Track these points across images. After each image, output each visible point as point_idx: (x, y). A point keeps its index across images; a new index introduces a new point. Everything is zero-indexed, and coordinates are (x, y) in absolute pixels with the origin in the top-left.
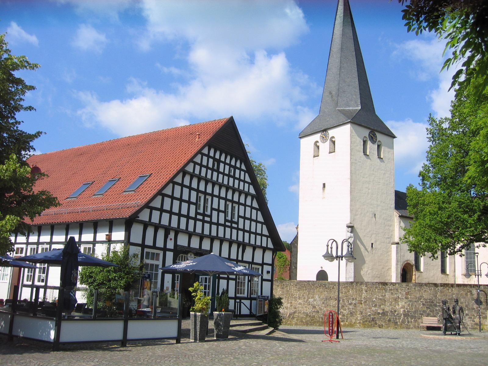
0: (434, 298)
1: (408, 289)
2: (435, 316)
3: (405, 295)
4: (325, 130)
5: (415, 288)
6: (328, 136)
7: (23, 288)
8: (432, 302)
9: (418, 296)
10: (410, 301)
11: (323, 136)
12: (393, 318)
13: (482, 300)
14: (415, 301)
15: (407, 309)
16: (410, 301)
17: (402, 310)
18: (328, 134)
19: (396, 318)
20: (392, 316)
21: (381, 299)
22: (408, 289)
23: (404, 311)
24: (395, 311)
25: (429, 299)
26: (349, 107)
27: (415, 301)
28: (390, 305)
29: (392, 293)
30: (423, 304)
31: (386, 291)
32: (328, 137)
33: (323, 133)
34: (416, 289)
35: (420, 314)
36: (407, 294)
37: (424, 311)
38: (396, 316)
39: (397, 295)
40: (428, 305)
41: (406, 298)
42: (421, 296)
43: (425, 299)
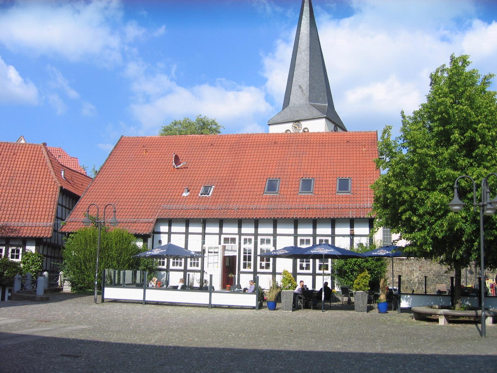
0: (440, 270)
1: (421, 263)
2: (442, 284)
3: (418, 268)
4: (298, 121)
5: (427, 263)
6: (301, 126)
7: (241, 275)
8: (440, 273)
9: (429, 268)
10: (423, 272)
11: (296, 126)
12: (410, 286)
13: (474, 271)
14: (427, 273)
15: (420, 278)
16: (423, 272)
17: (416, 279)
18: (301, 125)
19: (412, 286)
20: (408, 284)
21: (398, 271)
22: (421, 263)
23: (419, 280)
24: (411, 280)
25: (437, 271)
26: (319, 102)
27: (427, 273)
28: (406, 275)
29: (408, 267)
30: (433, 275)
31: (403, 265)
32: (301, 128)
33: (295, 124)
34: (428, 263)
35: (432, 282)
36: (420, 267)
37: (434, 280)
38: (412, 284)
39: (412, 268)
40: (436, 275)
41: (420, 270)
42: (431, 269)
43: (434, 271)
